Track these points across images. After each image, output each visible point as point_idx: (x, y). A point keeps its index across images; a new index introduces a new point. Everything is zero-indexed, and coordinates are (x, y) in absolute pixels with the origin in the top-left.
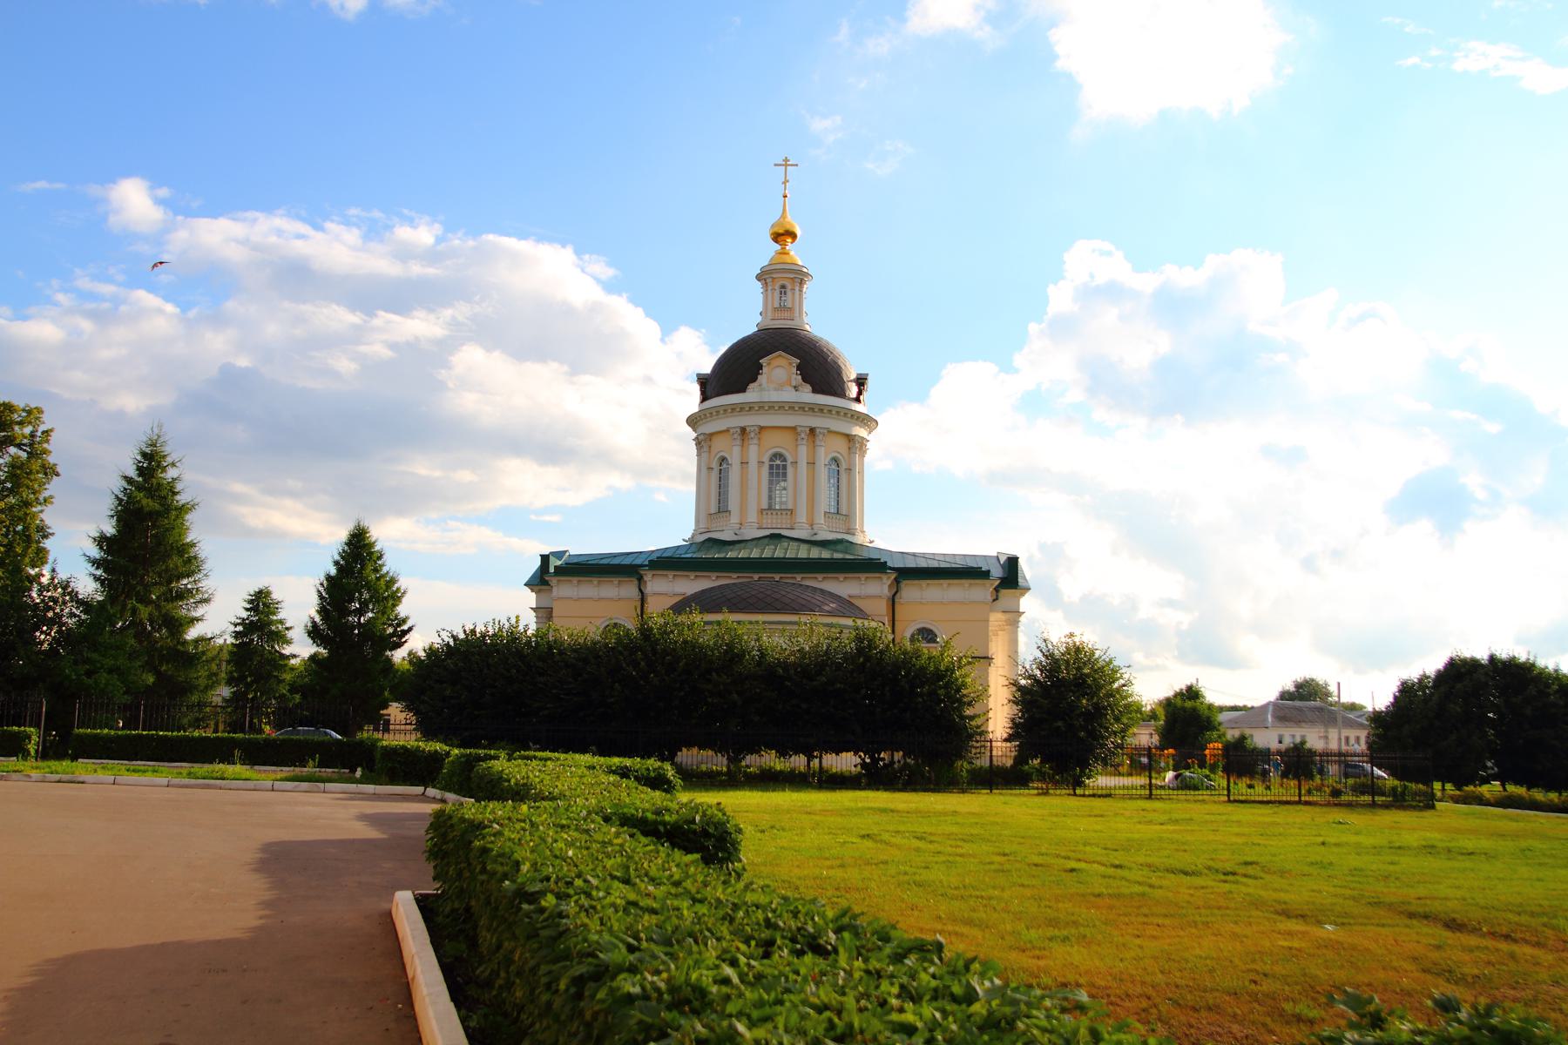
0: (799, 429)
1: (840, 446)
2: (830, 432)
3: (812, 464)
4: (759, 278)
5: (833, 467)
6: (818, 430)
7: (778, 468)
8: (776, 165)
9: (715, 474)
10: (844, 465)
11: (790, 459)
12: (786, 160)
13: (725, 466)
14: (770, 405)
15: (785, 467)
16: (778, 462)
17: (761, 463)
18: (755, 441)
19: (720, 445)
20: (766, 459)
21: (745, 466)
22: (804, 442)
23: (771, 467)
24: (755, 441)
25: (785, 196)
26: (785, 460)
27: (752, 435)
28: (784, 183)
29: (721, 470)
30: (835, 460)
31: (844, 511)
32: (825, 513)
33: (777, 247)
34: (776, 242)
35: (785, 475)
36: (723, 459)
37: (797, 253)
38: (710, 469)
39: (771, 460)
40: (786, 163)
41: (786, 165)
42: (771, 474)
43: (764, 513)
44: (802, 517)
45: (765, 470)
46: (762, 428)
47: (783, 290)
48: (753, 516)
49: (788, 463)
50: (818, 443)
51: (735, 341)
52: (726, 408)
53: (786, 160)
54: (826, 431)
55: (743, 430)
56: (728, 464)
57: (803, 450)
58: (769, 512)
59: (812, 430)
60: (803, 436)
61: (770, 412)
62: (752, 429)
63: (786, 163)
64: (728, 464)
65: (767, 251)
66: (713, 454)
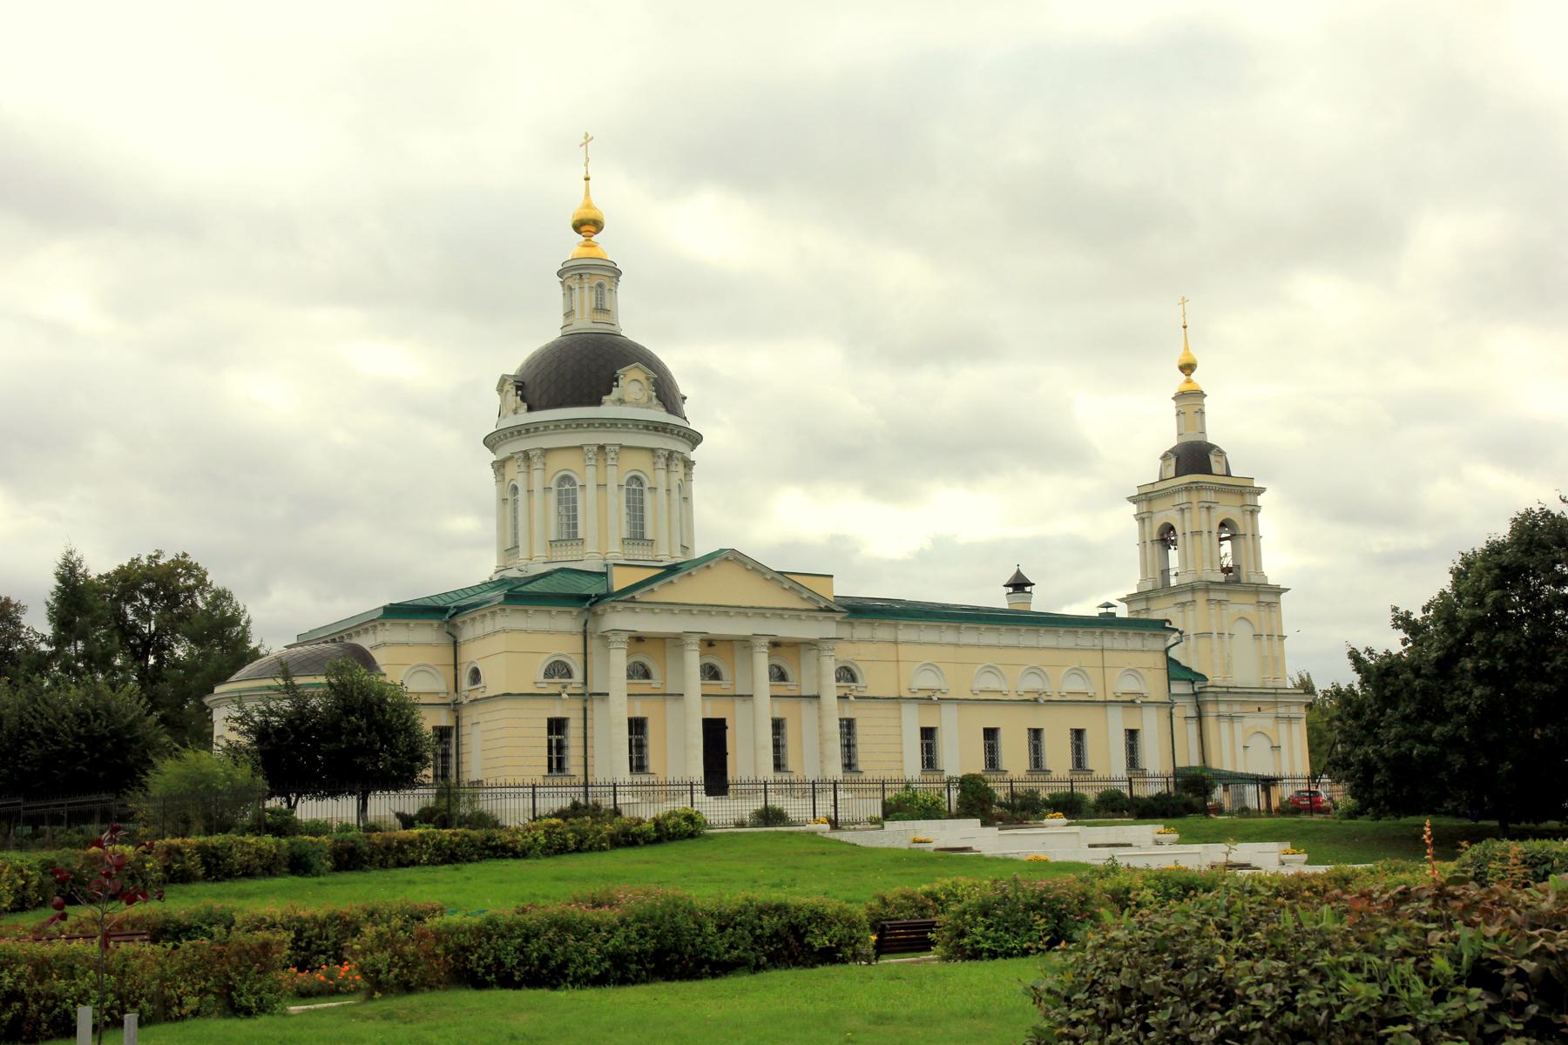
0: (585, 448)
1: (641, 463)
2: (622, 447)
3: (601, 486)
4: (560, 274)
7: (566, 490)
10: (647, 484)
11: (579, 483)
14: (568, 423)
16: (567, 487)
17: (547, 489)
18: (540, 466)
19: (512, 471)
20: (553, 484)
22: (593, 462)
23: (560, 493)
25: (587, 179)
27: (535, 459)
28: (586, 165)
30: (637, 479)
31: (649, 535)
32: (623, 540)
33: (580, 238)
34: (580, 233)
36: (515, 488)
37: (607, 245)
38: (505, 500)
42: (560, 502)
43: (553, 545)
45: (553, 497)
46: (546, 452)
48: (539, 552)
49: (578, 487)
50: (609, 462)
52: (519, 429)
54: (617, 448)
55: (526, 456)
57: (591, 471)
58: (569, 544)
59: (602, 448)
61: (579, 430)
62: (534, 453)
65: (572, 247)
66: (508, 478)
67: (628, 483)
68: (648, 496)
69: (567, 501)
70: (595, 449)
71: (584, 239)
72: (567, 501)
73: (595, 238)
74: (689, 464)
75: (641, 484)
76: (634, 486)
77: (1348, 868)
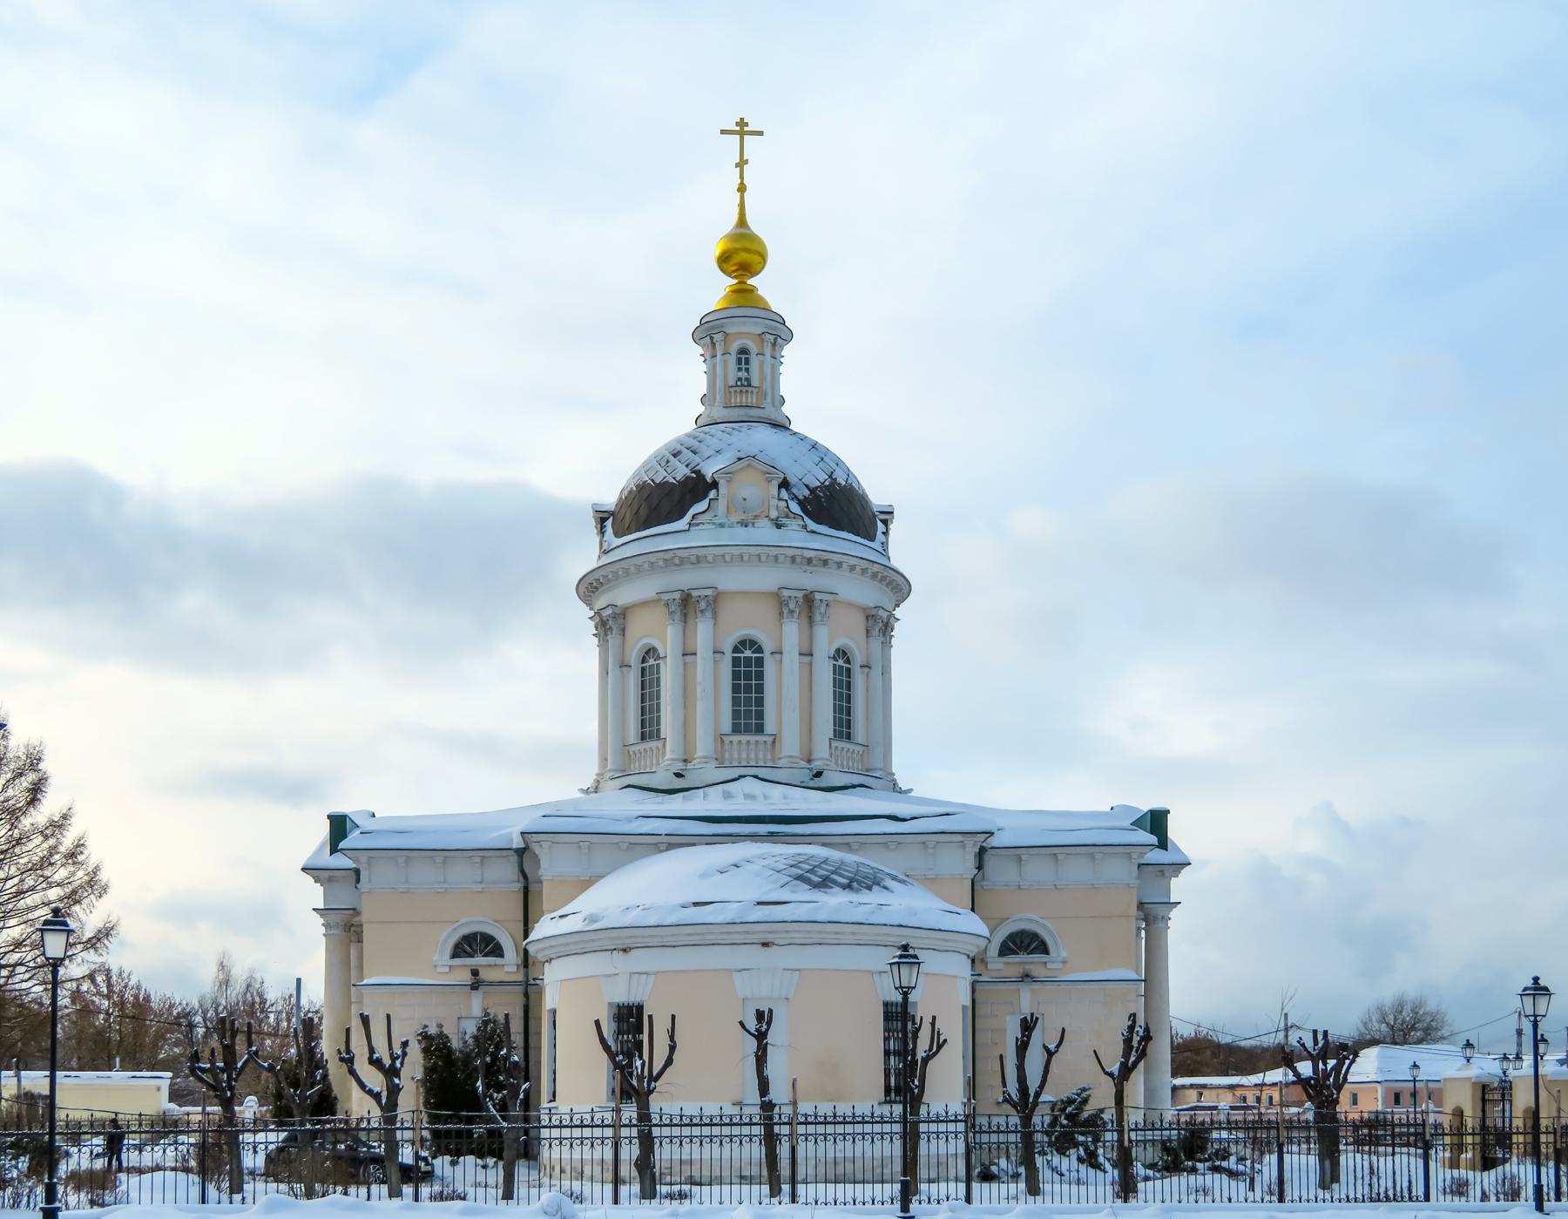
5: (840, 662)
6: (818, 596)
8: (723, 132)
9: (633, 679)
10: (858, 658)
11: (768, 646)
12: (742, 123)
13: (652, 662)
15: (760, 662)
16: (748, 653)
18: (708, 614)
20: (728, 647)
24: (708, 614)
26: (760, 650)
27: (703, 605)
29: (643, 670)
35: (760, 676)
36: (650, 652)
38: (624, 665)
39: (736, 650)
40: (742, 129)
41: (742, 134)
42: (736, 676)
47: (743, 356)
50: (817, 617)
51: (657, 448)
53: (742, 123)
56: (658, 658)
59: (809, 601)
60: (792, 605)
63: (742, 129)
64: (658, 658)
69: (748, 676)
70: (800, 594)
72: (748, 676)
76: (840, 662)
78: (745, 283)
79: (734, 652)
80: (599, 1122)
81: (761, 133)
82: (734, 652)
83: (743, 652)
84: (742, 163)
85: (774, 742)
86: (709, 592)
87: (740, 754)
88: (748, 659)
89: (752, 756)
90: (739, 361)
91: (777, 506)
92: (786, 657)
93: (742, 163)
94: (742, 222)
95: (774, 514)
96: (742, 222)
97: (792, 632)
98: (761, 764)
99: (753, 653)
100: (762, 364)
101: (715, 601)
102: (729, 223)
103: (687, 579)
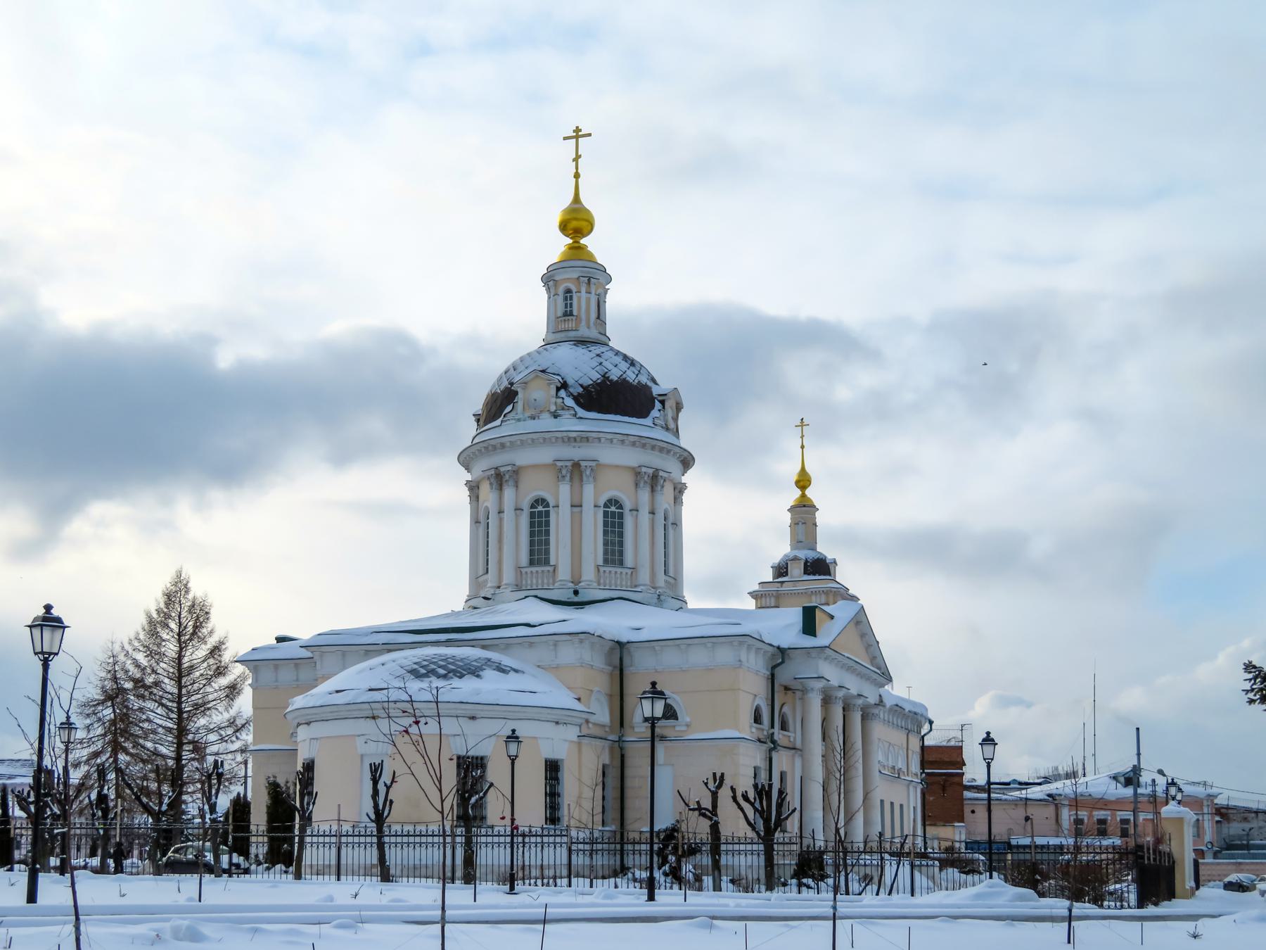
3: (577, 505)
6: (583, 464)
8: (565, 138)
12: (577, 130)
16: (540, 508)
17: (518, 509)
20: (526, 504)
21: (501, 514)
23: (532, 515)
24: (511, 483)
26: (548, 505)
39: (532, 506)
40: (578, 134)
42: (532, 525)
44: (564, 573)
47: (568, 295)
49: (551, 509)
53: (577, 130)
59: (576, 465)
63: (578, 134)
67: (606, 506)
68: (629, 522)
71: (571, 241)
72: (540, 524)
73: (583, 241)
74: (680, 489)
75: (621, 507)
76: (613, 509)
77: (1239, 842)
78: (578, 242)
79: (531, 508)
80: (419, 833)
81: (590, 135)
82: (531, 508)
83: (537, 508)
84: (577, 158)
85: (554, 570)
86: (593, 464)
87: (532, 581)
88: (613, 513)
89: (534, 581)
90: (566, 299)
91: (556, 403)
92: (512, 507)
93: (577, 158)
94: (577, 199)
95: (553, 408)
96: (577, 199)
97: (565, 490)
98: (535, 587)
99: (543, 507)
100: (579, 298)
101: (516, 472)
102: (568, 200)
103: (499, 459)
